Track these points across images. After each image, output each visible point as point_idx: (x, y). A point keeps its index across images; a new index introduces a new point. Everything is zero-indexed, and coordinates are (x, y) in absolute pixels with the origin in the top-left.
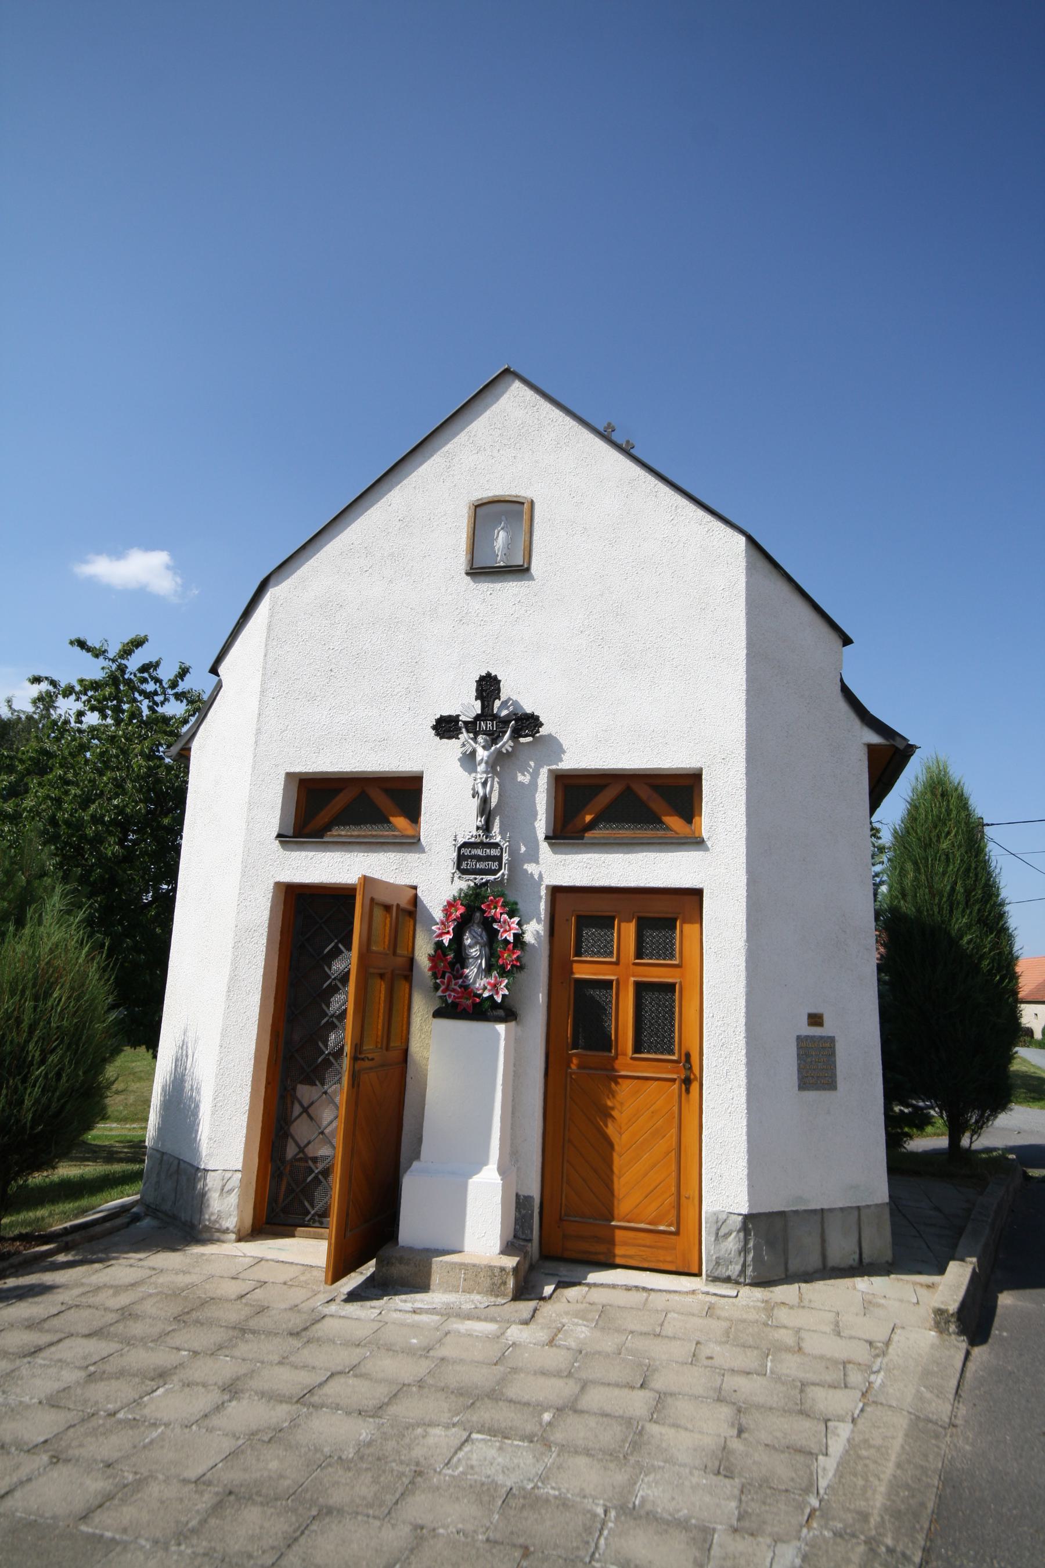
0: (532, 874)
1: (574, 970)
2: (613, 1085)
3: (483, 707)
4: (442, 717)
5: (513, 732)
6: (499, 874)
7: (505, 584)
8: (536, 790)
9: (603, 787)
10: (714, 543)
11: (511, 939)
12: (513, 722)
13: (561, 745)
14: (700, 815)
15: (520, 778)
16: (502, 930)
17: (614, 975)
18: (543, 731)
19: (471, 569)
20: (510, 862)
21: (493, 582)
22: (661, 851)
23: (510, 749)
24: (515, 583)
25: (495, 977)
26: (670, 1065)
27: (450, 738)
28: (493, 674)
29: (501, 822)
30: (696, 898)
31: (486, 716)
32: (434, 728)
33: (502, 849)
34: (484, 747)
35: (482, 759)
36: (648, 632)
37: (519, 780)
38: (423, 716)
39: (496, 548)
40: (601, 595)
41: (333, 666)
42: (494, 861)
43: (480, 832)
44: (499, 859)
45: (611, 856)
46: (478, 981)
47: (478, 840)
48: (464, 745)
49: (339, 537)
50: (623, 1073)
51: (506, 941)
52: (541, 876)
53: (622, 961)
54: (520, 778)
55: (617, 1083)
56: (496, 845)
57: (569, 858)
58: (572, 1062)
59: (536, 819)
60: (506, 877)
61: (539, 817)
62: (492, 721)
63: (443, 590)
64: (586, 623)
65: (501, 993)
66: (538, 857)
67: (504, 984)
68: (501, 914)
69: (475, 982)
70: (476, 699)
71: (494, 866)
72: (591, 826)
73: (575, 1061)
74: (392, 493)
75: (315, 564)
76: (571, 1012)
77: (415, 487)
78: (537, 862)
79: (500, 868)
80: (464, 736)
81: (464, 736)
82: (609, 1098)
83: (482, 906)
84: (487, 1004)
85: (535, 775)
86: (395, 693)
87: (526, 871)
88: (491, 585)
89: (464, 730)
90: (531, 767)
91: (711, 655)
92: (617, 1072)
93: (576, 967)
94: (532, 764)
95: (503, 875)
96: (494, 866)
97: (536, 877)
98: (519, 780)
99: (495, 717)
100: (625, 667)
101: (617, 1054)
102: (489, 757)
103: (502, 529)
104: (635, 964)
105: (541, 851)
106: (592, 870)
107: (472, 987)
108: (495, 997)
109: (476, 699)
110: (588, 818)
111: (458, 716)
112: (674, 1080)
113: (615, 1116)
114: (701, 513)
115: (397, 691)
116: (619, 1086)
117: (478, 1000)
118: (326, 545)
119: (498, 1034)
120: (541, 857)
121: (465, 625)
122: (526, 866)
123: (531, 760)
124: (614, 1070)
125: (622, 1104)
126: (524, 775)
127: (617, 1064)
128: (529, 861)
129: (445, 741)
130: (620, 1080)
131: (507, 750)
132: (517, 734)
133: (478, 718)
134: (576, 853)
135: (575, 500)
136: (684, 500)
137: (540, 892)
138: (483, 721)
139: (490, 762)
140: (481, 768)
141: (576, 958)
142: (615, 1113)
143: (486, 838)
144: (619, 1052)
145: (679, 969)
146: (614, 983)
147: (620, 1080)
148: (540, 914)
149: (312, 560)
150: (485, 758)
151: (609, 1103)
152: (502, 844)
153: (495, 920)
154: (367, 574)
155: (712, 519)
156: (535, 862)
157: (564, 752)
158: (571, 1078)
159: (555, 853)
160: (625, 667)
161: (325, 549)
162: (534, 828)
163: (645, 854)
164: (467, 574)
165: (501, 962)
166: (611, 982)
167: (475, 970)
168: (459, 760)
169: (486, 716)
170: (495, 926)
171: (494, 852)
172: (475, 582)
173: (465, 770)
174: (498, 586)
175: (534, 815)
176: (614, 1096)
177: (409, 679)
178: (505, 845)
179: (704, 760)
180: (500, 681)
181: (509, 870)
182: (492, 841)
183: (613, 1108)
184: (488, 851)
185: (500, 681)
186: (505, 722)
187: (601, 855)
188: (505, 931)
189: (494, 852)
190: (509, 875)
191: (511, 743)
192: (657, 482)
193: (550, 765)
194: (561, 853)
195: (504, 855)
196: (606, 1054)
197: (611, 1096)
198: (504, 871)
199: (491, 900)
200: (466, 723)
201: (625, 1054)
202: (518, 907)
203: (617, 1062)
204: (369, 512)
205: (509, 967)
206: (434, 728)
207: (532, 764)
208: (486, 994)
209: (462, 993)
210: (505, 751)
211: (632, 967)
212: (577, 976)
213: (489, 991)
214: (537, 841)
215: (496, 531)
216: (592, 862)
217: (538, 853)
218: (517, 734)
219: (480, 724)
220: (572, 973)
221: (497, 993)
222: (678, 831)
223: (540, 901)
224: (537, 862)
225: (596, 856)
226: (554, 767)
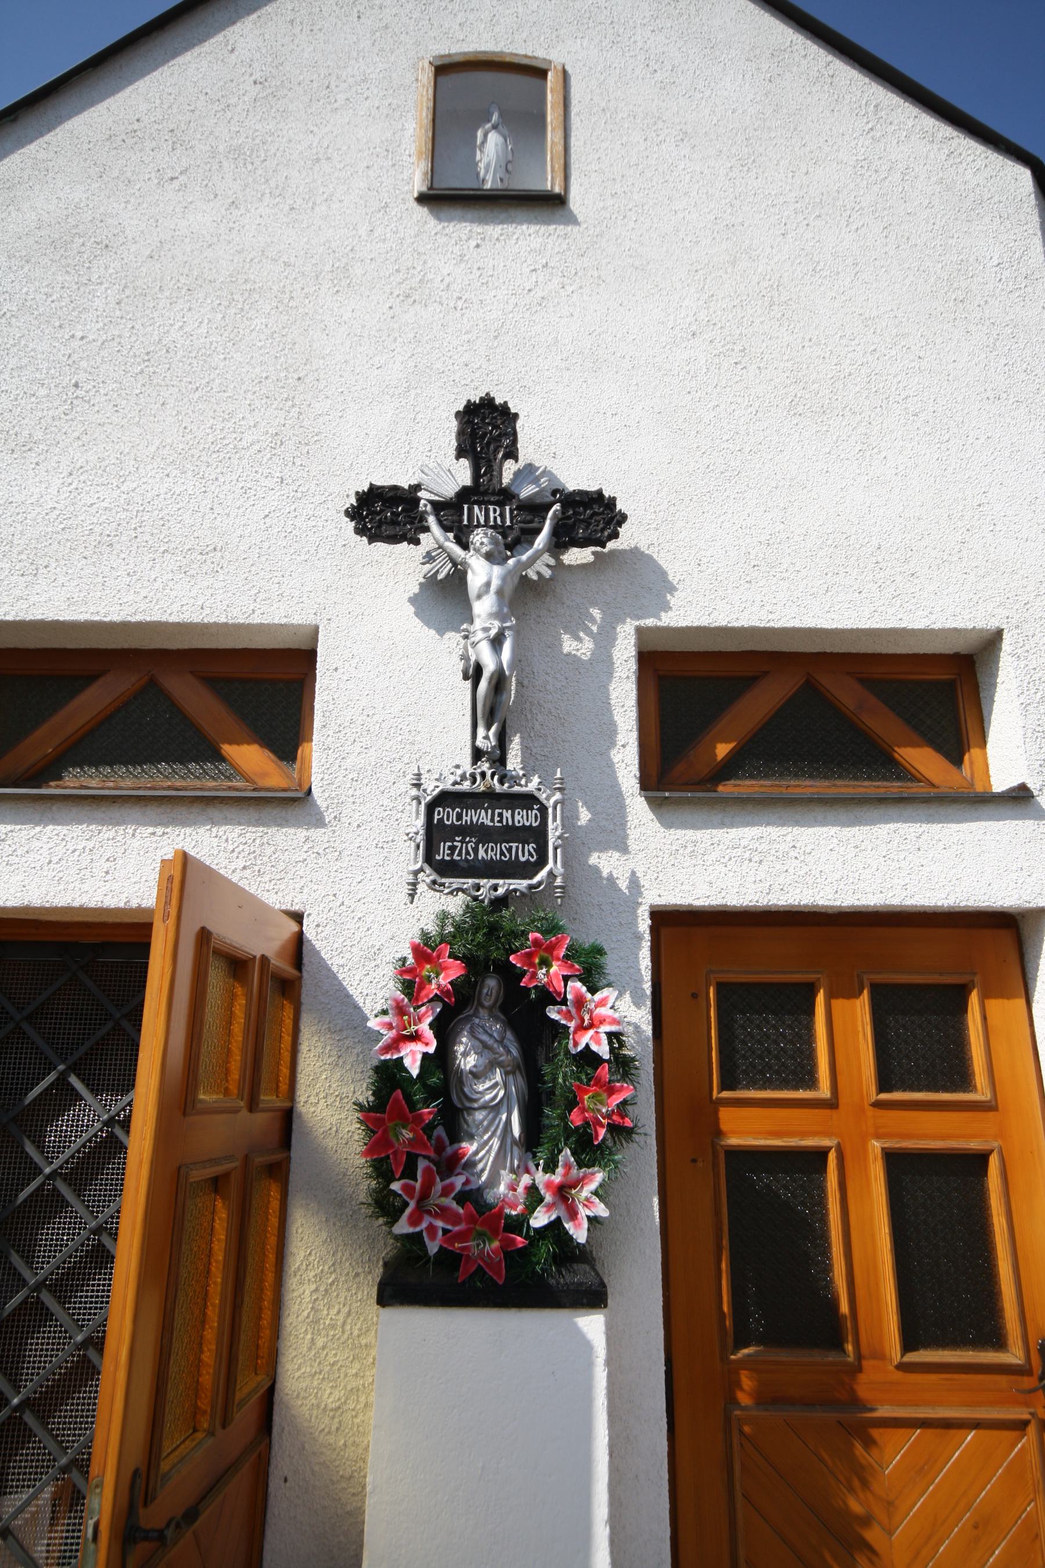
0: (611, 879)
1: (724, 1127)
2: (859, 1449)
3: (476, 475)
4: (372, 487)
5: (555, 532)
6: (543, 874)
7: (510, 228)
8: (610, 673)
9: (750, 681)
10: (967, 178)
11: (603, 1050)
12: (557, 507)
13: (664, 574)
14: (983, 742)
15: (568, 645)
16: (572, 1025)
17: (827, 1134)
18: (627, 538)
19: (430, 188)
20: (565, 843)
21: (481, 221)
22: (930, 820)
23: (547, 573)
24: (533, 228)
25: (568, 1167)
26: (1003, 1380)
27: (394, 539)
28: (499, 401)
29: (525, 749)
30: (1005, 937)
31: (485, 493)
32: (353, 514)
33: (543, 810)
34: (489, 557)
35: (488, 584)
36: (844, 341)
37: (566, 649)
38: (318, 499)
39: (482, 165)
40: (733, 264)
41: (82, 376)
42: (525, 842)
43: (485, 766)
44: (538, 835)
45: (811, 831)
46: (506, 1177)
47: (480, 787)
48: (429, 558)
49: (105, 104)
50: (884, 1411)
51: (589, 1058)
52: (634, 882)
53: (843, 1100)
54: (568, 645)
55: (869, 1443)
56: (528, 800)
57: (704, 837)
58: (739, 1385)
59: (613, 744)
60: (559, 881)
61: (621, 739)
62: (501, 504)
63: (363, 231)
64: (702, 315)
65: (583, 1212)
66: (626, 837)
67: (593, 1186)
68: (566, 979)
69: (494, 1180)
70: (458, 458)
71: (526, 853)
72: (728, 770)
73: (747, 1381)
74: (237, 28)
75: (42, 155)
76: (725, 1242)
77: (292, 22)
78: (623, 848)
79: (542, 861)
80: (435, 536)
81: (435, 536)
82: (851, 1489)
83: (512, 958)
84: (546, 1249)
85: (605, 640)
86: (244, 443)
87: (596, 870)
88: (478, 229)
89: (431, 520)
90: (593, 620)
91: (990, 394)
92: (872, 1410)
93: (727, 1117)
94: (596, 613)
95: (551, 875)
96: (526, 853)
97: (623, 884)
98: (566, 649)
99: (505, 496)
100: (800, 409)
101: (859, 1356)
102: (504, 579)
103: (495, 127)
104: (878, 1105)
105: (632, 820)
106: (764, 866)
107: (490, 1197)
108: (568, 1226)
109: (458, 458)
110: (722, 750)
111: (417, 487)
112: (1021, 1426)
113: (876, 1546)
114: (929, 122)
115: (248, 438)
116: (875, 1452)
117: (520, 1241)
118: (70, 117)
119: (587, 1346)
120: (633, 834)
121: (417, 306)
122: (594, 859)
123: (594, 604)
124: (856, 1403)
125: (889, 1505)
126: (579, 639)
127: (864, 1386)
128: (603, 847)
129: (381, 547)
130: (875, 1433)
131: (538, 573)
132: (561, 540)
133: (465, 495)
134: (722, 825)
135: (658, 76)
136: (890, 94)
137: (634, 922)
138: (479, 503)
139: (508, 590)
140: (483, 607)
141: (725, 1094)
142: (873, 1535)
143: (501, 782)
144: (865, 1350)
145: (991, 1114)
146: (832, 1156)
147: (875, 1433)
148: (640, 981)
149: (32, 147)
150: (495, 583)
151: (855, 1506)
152: (543, 797)
153: (548, 997)
154: (176, 184)
155: (955, 133)
156: (617, 848)
157: (672, 589)
158: (741, 1432)
159: (667, 825)
160: (800, 409)
161: (69, 125)
162: (610, 765)
163: (892, 826)
164: (423, 199)
165: (575, 1119)
166: (821, 1154)
167: (496, 1143)
168: (413, 600)
169: (485, 493)
170: (553, 1013)
171: (523, 818)
172: (439, 219)
173: (428, 623)
174: (494, 230)
175: (610, 732)
176: (865, 1484)
177: (282, 414)
178: (551, 799)
179: (1006, 613)
180: (516, 416)
181: (565, 864)
182: (516, 789)
183: (866, 1521)
184: (507, 814)
185: (516, 416)
186: (536, 509)
187: (784, 830)
188: (582, 1028)
189: (523, 818)
190: (565, 877)
191: (548, 559)
192: (830, 58)
193: (639, 618)
194: (684, 826)
195: (551, 825)
196: (832, 1357)
197: (856, 1483)
198: (554, 864)
199: (536, 943)
200: (438, 507)
201: (880, 1356)
202: (603, 960)
203: (862, 1378)
204: (180, 60)
205: (602, 1132)
206: (353, 514)
207: (596, 613)
208: (540, 1219)
209: (470, 1219)
210: (535, 577)
211: (870, 1112)
212: (733, 1141)
213: (550, 1207)
214: (618, 796)
215: (480, 133)
216: (764, 847)
217: (623, 824)
218: (561, 540)
219: (471, 511)
220: (719, 1133)
221: (573, 1215)
222: (936, 782)
223: (639, 948)
224: (623, 848)
225: (773, 832)
226: (650, 622)
